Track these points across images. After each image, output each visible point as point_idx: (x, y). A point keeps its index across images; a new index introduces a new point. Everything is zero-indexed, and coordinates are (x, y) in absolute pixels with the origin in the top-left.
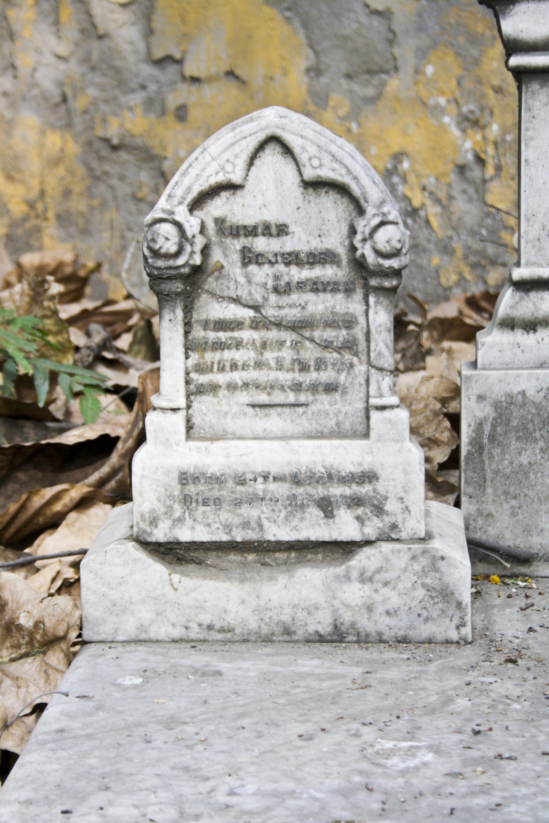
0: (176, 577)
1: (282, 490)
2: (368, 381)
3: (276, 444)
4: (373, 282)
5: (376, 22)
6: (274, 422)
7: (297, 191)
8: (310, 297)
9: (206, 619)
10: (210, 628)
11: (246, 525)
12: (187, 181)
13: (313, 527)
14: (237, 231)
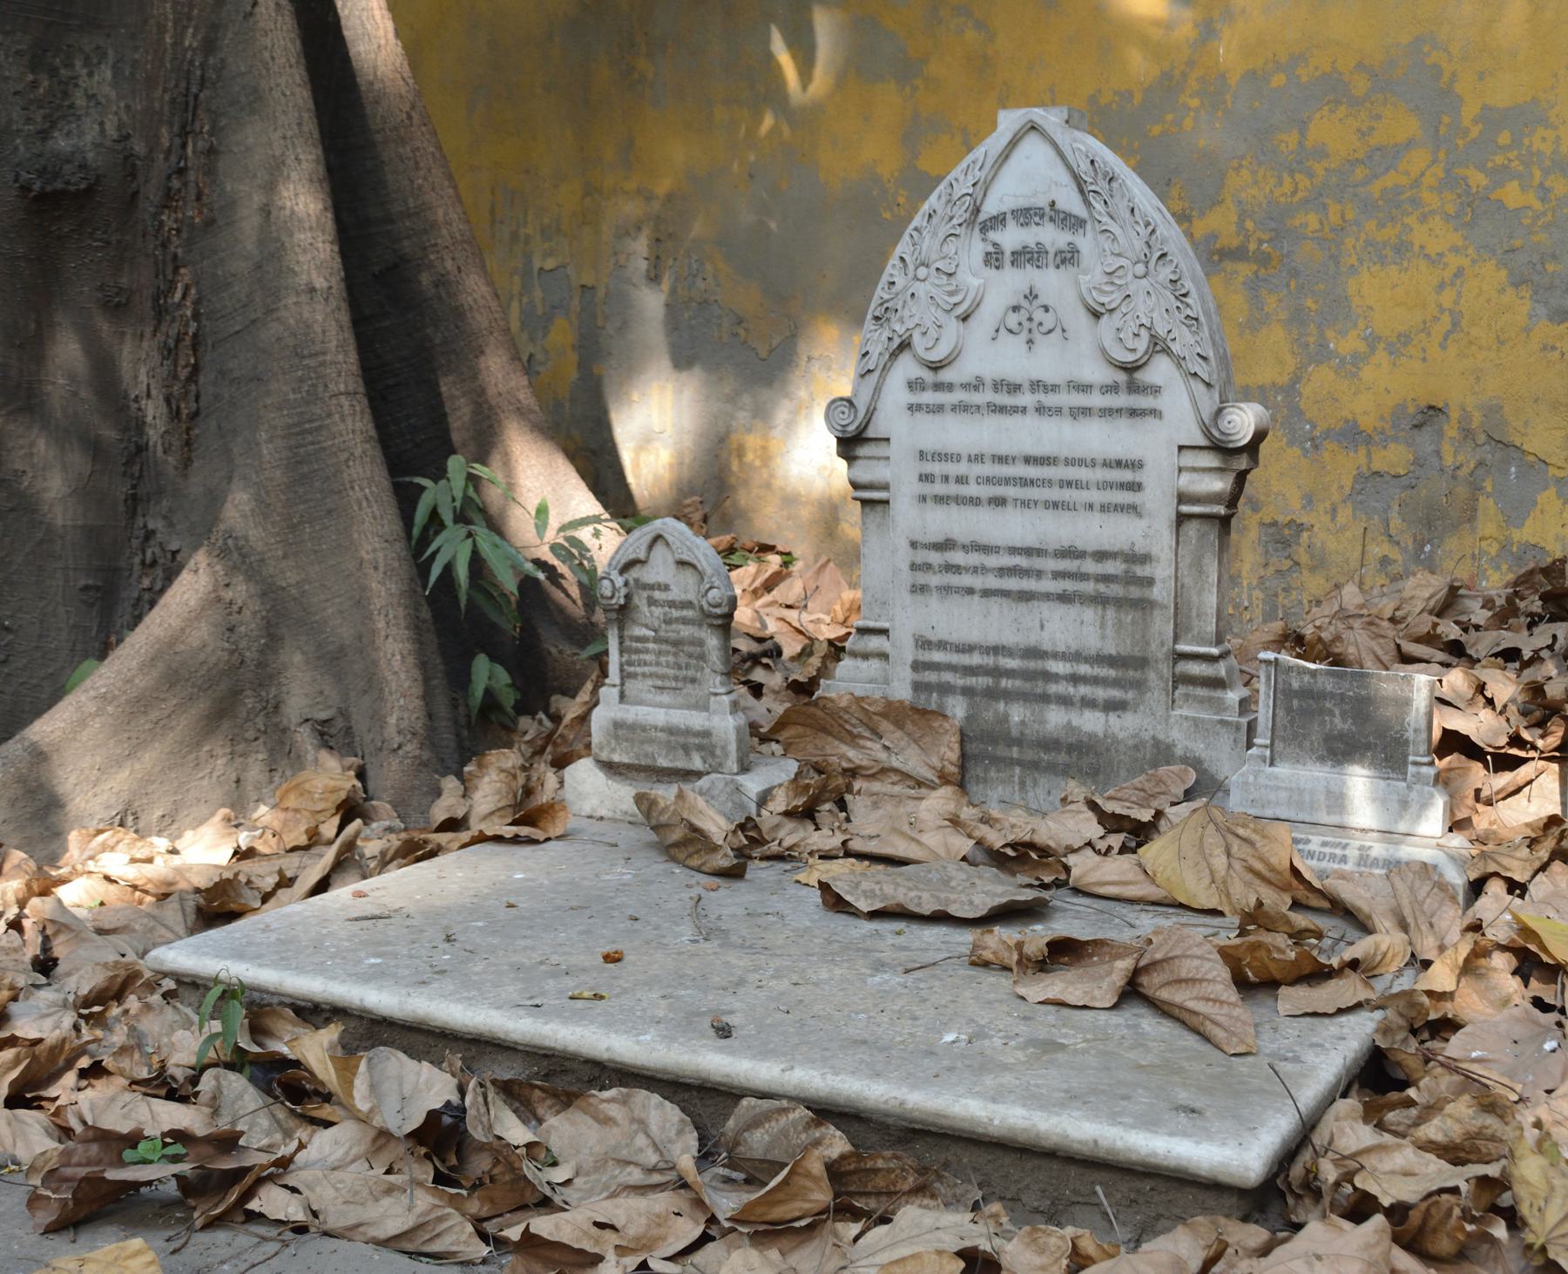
6: (665, 698)
7: (673, 566)
8: (681, 627)
11: (646, 755)
13: (680, 764)
14: (646, 587)
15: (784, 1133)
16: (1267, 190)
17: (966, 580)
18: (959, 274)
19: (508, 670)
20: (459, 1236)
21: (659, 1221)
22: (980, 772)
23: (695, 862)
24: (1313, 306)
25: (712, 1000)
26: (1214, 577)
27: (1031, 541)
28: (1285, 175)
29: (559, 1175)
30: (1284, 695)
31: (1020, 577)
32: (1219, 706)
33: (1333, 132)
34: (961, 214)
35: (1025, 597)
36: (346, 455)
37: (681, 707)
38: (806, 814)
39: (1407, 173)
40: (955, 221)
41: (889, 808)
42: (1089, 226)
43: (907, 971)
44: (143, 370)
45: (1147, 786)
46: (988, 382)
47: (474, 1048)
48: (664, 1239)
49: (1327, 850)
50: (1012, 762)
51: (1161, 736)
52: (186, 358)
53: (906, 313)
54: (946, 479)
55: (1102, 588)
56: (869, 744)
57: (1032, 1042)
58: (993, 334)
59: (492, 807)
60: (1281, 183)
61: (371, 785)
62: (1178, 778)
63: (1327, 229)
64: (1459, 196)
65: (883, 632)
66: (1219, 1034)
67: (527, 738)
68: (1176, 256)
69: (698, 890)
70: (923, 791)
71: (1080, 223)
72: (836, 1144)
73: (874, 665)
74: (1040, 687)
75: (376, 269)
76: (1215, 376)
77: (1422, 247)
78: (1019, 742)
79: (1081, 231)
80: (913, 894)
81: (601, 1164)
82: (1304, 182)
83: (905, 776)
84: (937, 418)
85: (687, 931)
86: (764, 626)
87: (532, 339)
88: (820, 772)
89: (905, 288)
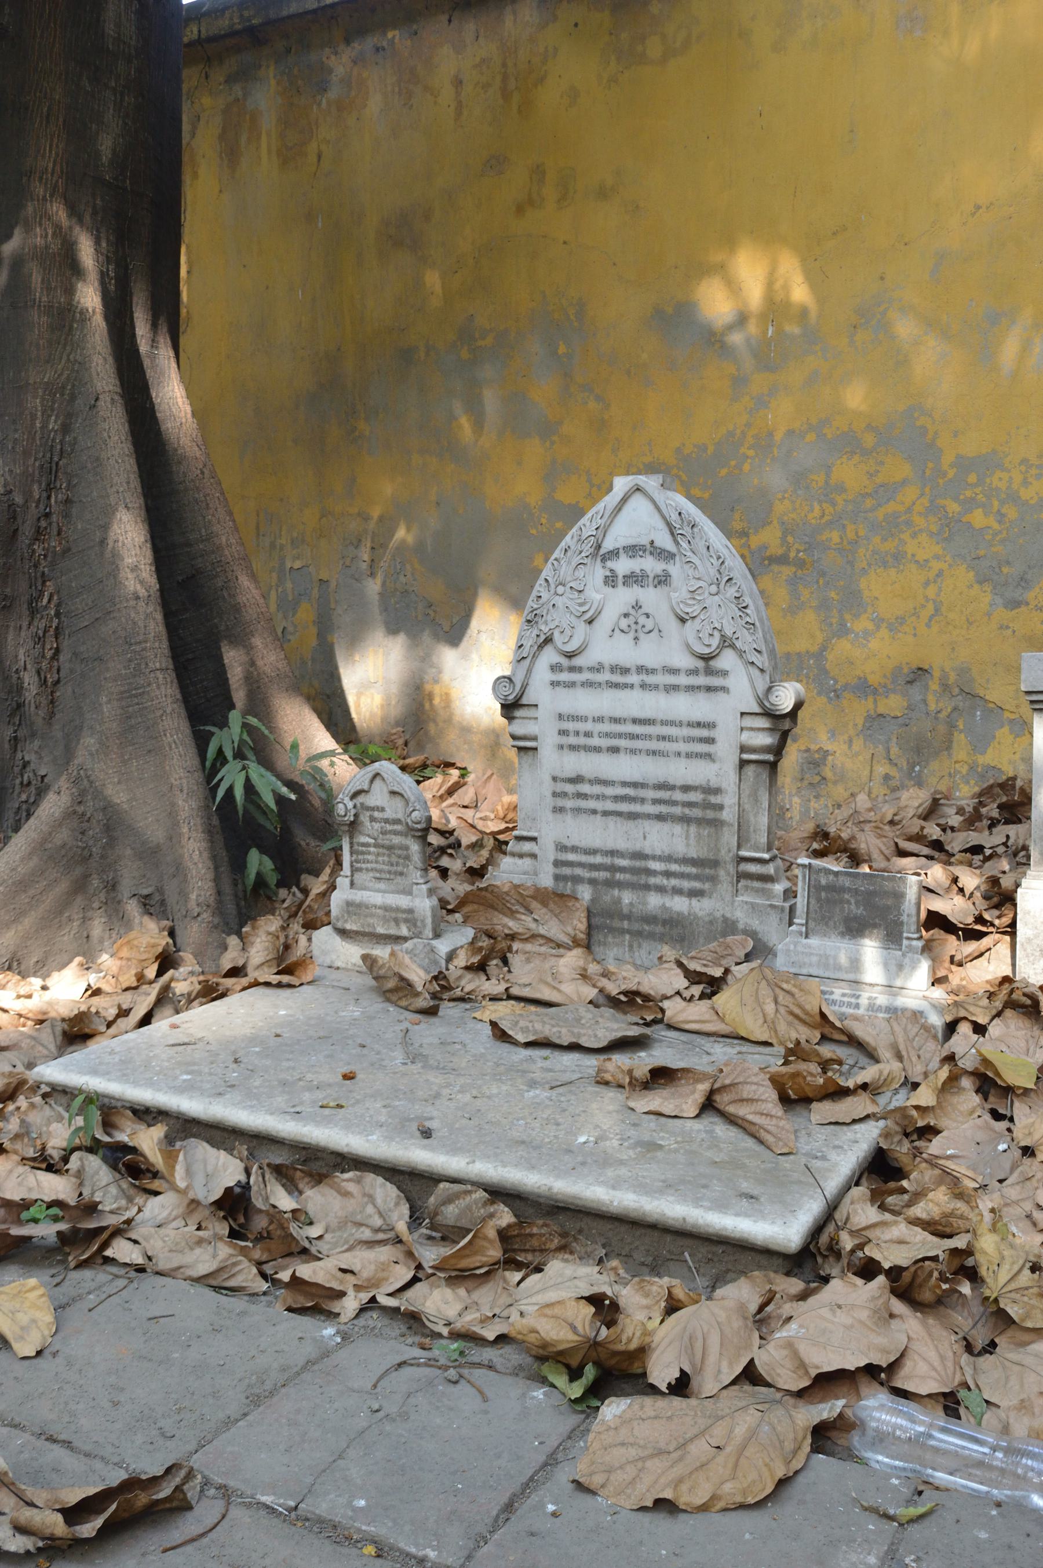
6: (382, 886)
7: (387, 795)
11: (369, 925)
13: (393, 931)
15: (469, 1208)
17: (592, 804)
19: (271, 858)
20: (247, 1276)
21: (383, 1267)
22: (601, 938)
23: (404, 1003)
24: (836, 597)
25: (417, 1109)
26: (766, 804)
27: (637, 777)
29: (314, 1232)
30: (815, 888)
31: (628, 802)
34: (587, 549)
35: (633, 816)
36: (159, 713)
37: (393, 892)
38: (480, 968)
41: (537, 962)
42: (677, 558)
43: (552, 1088)
44: (22, 651)
45: (718, 950)
46: (607, 666)
47: (256, 1141)
48: (386, 1279)
50: (623, 932)
51: (728, 915)
52: (50, 643)
53: (549, 618)
54: (577, 733)
55: (687, 811)
56: (523, 917)
57: (640, 1143)
58: (610, 633)
59: (262, 960)
61: (179, 940)
62: (742, 945)
65: (534, 839)
66: (770, 1139)
67: (285, 905)
68: (739, 580)
69: (406, 1025)
70: (562, 951)
71: (669, 556)
72: (505, 1217)
73: (527, 861)
74: (643, 879)
75: (180, 578)
76: (767, 664)
78: (629, 917)
80: (555, 1030)
81: (343, 1224)
83: (549, 940)
84: (571, 691)
85: (399, 1056)
86: (448, 821)
87: (285, 617)
88: (490, 936)
89: (549, 601)
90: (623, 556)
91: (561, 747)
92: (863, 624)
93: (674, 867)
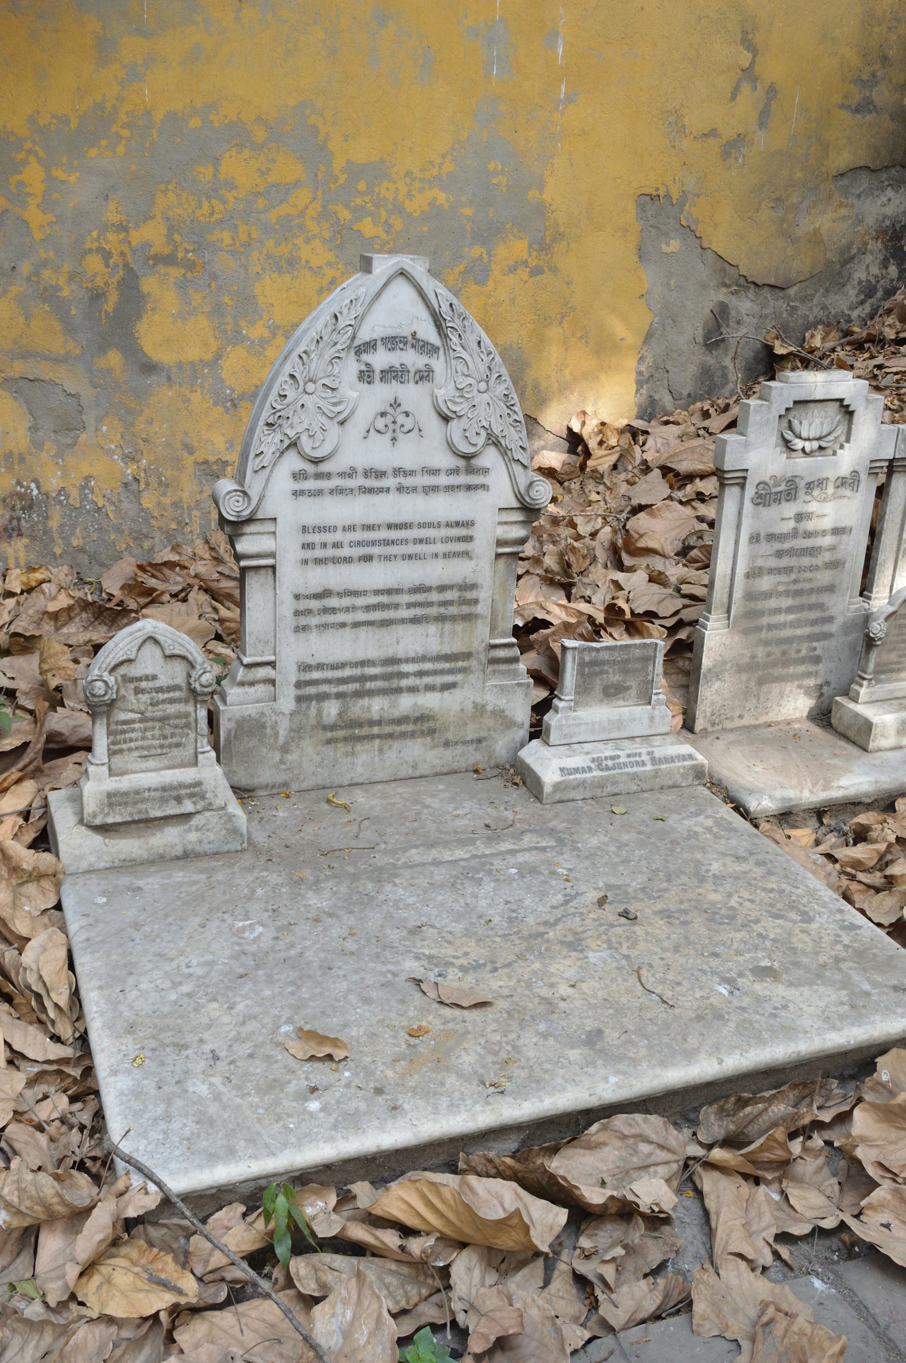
0: (107, 841)
1: (157, 794)
2: (196, 741)
3: (153, 774)
4: (199, 698)
5: (70, 400)
6: (151, 763)
7: (161, 660)
8: (168, 706)
9: (122, 857)
10: (124, 860)
11: (140, 812)
12: (108, 660)
13: (173, 809)
14: (132, 680)
16: (190, 211)
17: (340, 618)
18: (342, 391)
24: (230, 303)
27: (391, 583)
28: (204, 199)
31: (382, 612)
32: (515, 674)
33: (238, 168)
39: (295, 206)
40: (339, 347)
42: (441, 352)
49: (632, 759)
50: (372, 737)
51: (479, 700)
54: (324, 545)
55: (442, 610)
60: (200, 207)
63: (238, 245)
64: (332, 226)
65: (272, 664)
71: (436, 349)
74: (395, 683)
77: (307, 262)
78: (379, 723)
79: (435, 355)
82: (219, 207)
84: (317, 500)
90: (381, 348)
91: (305, 562)
92: (258, 331)
93: (428, 666)
